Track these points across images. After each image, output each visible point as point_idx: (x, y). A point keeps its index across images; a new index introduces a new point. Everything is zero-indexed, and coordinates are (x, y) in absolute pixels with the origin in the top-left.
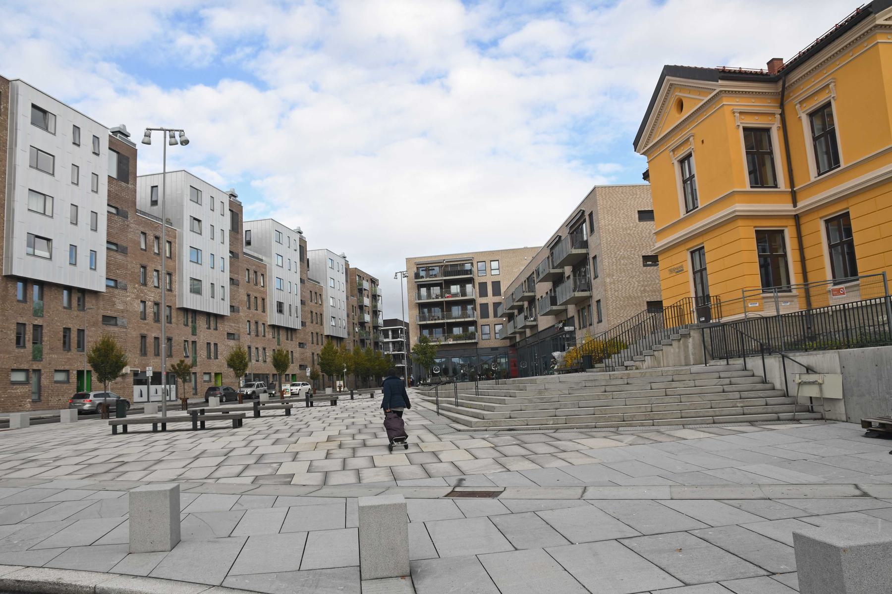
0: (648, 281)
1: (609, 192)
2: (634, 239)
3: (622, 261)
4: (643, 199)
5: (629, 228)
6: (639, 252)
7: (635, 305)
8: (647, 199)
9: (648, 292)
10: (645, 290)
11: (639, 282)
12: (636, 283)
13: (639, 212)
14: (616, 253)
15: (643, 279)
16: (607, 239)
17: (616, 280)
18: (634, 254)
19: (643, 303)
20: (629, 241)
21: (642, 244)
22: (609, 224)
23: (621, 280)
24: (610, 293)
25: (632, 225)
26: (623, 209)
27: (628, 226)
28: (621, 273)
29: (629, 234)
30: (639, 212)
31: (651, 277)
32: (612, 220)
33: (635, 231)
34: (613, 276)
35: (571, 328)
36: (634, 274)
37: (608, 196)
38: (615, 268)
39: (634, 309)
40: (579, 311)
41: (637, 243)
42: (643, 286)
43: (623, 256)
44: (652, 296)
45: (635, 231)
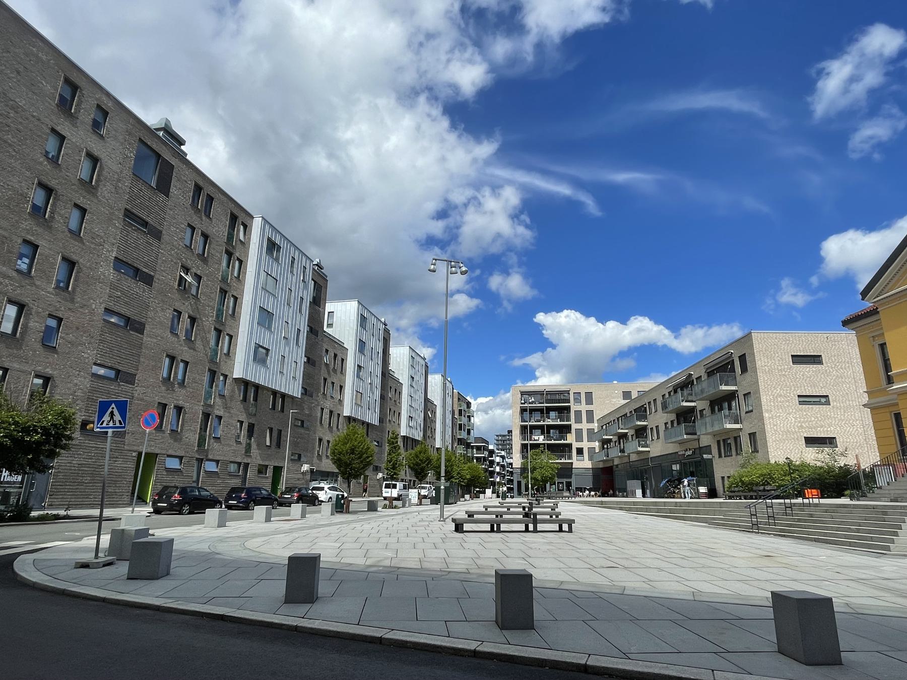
0: (804, 418)
1: (764, 338)
2: (789, 379)
3: (779, 399)
4: (796, 345)
5: (784, 370)
6: (795, 392)
7: (794, 439)
8: (799, 345)
9: (805, 428)
10: (801, 426)
11: (796, 418)
12: (793, 419)
13: (792, 356)
14: (773, 391)
15: (800, 416)
16: (764, 378)
17: (774, 415)
18: (790, 394)
19: (801, 438)
20: (784, 381)
21: (797, 385)
22: (765, 366)
23: (779, 416)
24: (769, 427)
25: (786, 367)
26: (778, 353)
27: (783, 367)
28: (778, 409)
29: (784, 375)
30: (792, 356)
31: (807, 414)
32: (768, 362)
33: (789, 372)
34: (771, 411)
35: (710, 456)
36: (791, 411)
37: (763, 341)
38: (773, 404)
39: (793, 443)
40: (718, 442)
41: (792, 384)
42: (799, 422)
43: (780, 394)
44: (809, 431)
45: (789, 372)
